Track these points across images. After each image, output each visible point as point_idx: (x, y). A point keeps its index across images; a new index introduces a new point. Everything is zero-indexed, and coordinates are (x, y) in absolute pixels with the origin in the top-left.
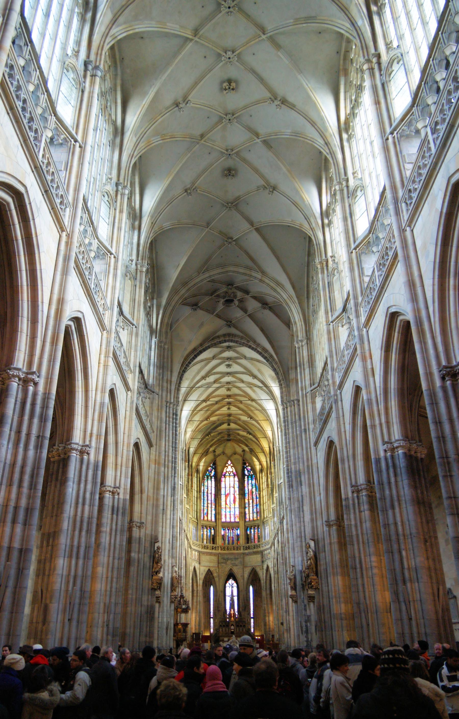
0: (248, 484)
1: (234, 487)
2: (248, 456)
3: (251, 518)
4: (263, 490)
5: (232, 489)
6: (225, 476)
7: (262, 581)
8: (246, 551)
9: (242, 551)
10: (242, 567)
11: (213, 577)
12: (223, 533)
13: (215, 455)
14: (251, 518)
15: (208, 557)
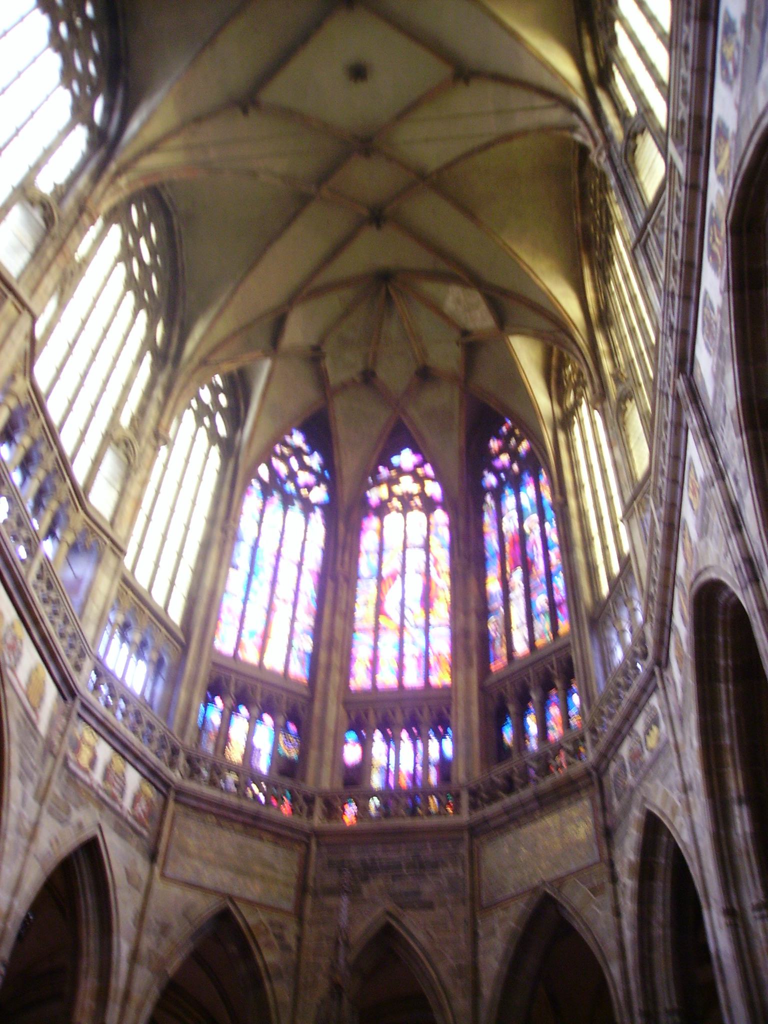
0: (499, 516)
1: (427, 547)
2: (486, 379)
3: (521, 647)
4: (578, 488)
5: (416, 558)
6: (382, 510)
7: (615, 969)
8: (494, 808)
9: (465, 817)
10: (463, 912)
11: (255, 979)
12: (352, 753)
13: (321, 379)
14: (521, 647)
15: (228, 840)
